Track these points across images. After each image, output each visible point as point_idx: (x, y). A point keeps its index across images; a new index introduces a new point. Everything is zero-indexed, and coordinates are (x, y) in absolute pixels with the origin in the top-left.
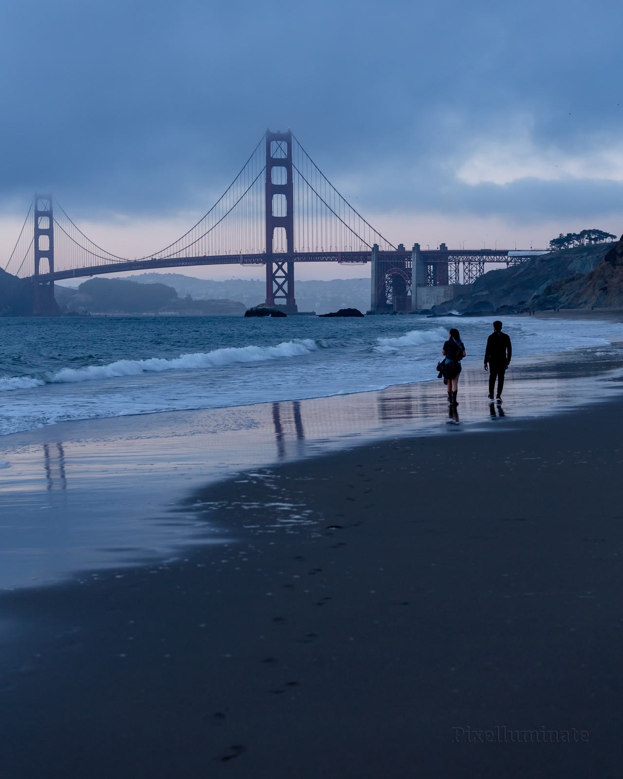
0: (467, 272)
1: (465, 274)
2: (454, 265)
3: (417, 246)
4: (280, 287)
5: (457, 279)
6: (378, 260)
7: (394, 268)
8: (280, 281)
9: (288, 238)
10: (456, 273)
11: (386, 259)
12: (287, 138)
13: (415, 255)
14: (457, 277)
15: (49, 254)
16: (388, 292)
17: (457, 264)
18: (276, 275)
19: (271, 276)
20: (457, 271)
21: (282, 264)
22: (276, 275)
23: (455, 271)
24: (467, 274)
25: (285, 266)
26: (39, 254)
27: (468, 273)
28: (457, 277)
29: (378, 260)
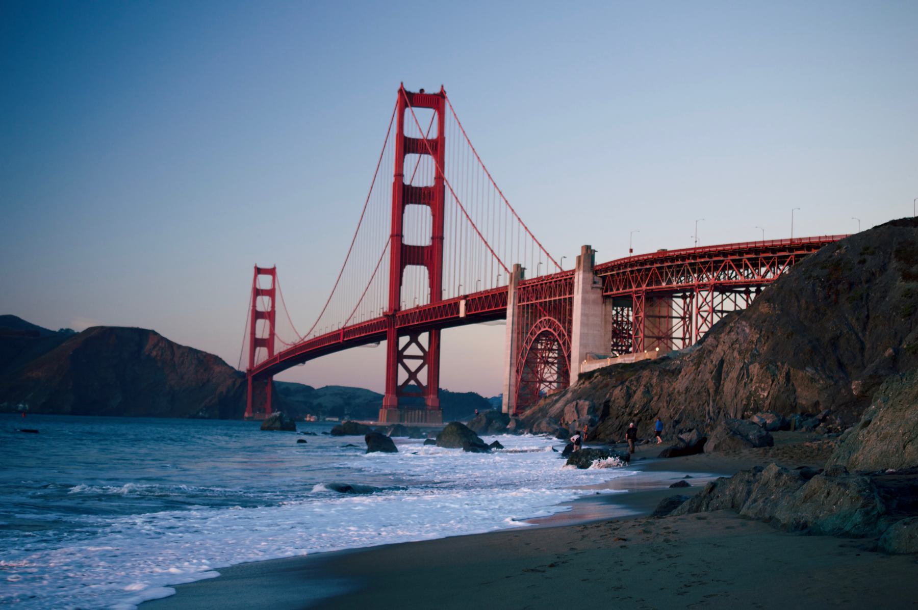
0: (705, 314)
1: (700, 321)
2: (680, 301)
3: (589, 253)
4: (413, 375)
5: (687, 341)
6: (519, 302)
7: (543, 319)
8: (413, 365)
9: (432, 285)
10: (685, 323)
11: (532, 297)
12: (436, 101)
13: (581, 276)
14: (687, 336)
15: (268, 343)
16: (542, 381)
17: (688, 300)
18: (406, 353)
19: (396, 357)
20: (686, 318)
21: (419, 333)
22: (406, 353)
23: (683, 318)
24: (705, 320)
25: (424, 338)
26: (256, 343)
27: (709, 319)
28: (687, 336)
29: (519, 302)
